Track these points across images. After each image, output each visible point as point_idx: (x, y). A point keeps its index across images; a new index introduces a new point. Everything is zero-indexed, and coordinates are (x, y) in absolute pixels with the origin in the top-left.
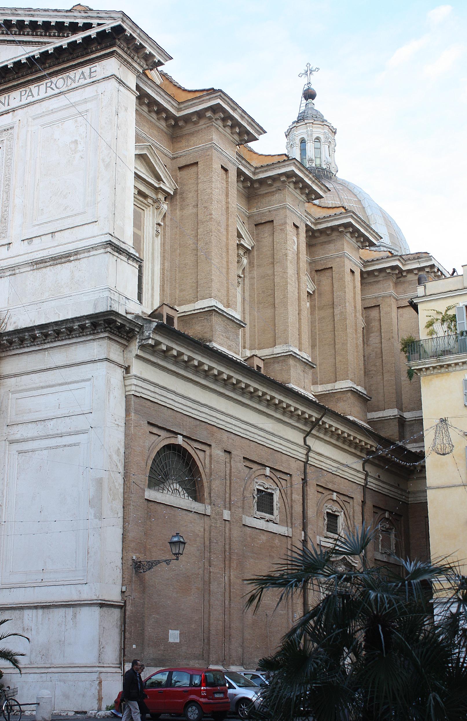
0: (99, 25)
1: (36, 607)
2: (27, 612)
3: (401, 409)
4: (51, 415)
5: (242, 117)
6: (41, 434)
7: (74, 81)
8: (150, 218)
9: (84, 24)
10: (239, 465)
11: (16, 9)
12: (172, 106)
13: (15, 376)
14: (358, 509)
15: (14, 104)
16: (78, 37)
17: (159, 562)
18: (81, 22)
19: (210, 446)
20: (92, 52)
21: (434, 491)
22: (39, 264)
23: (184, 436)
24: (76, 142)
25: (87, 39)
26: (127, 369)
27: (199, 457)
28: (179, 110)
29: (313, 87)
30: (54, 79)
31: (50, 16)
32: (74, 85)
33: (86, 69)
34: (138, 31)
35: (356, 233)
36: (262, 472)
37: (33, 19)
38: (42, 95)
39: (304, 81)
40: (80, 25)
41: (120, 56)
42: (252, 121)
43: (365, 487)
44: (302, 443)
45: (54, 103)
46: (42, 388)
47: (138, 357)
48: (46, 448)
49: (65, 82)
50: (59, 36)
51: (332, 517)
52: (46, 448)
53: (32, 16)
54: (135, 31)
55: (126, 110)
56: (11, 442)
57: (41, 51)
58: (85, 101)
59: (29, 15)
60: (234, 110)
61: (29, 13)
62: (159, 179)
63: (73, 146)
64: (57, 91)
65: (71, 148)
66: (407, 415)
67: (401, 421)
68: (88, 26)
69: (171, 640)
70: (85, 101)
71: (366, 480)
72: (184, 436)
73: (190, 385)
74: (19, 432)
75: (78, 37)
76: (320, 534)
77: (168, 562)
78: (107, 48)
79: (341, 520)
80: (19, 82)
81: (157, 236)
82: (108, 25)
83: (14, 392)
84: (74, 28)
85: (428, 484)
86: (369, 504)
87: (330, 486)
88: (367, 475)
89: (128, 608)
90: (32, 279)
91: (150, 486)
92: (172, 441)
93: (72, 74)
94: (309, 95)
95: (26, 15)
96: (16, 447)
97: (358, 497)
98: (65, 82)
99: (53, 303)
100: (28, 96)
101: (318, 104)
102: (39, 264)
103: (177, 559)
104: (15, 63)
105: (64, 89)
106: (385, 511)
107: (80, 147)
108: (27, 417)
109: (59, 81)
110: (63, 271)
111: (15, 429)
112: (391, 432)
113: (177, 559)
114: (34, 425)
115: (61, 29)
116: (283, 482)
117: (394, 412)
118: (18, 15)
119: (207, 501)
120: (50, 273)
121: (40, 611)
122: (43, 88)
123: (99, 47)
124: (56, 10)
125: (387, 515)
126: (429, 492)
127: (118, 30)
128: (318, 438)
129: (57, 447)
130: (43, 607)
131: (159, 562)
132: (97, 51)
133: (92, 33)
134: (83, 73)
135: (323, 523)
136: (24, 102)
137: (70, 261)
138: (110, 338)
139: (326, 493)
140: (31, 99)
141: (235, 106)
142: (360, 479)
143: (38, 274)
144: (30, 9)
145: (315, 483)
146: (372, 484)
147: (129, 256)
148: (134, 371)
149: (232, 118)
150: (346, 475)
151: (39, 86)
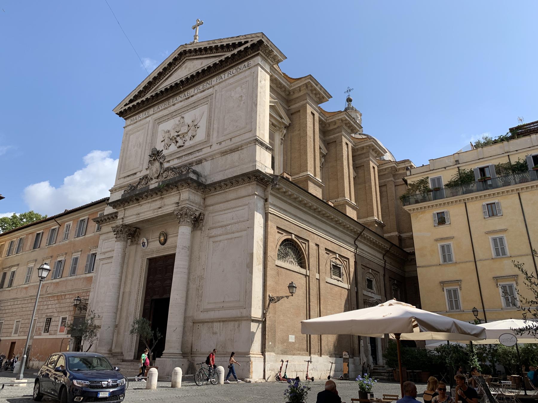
1: (220, 321)
2: (215, 324)
3: (399, 232)
4: (229, 222)
5: (321, 89)
7: (241, 69)
8: (278, 138)
10: (322, 252)
11: (214, 40)
12: (288, 85)
13: (212, 205)
14: (382, 278)
15: (213, 83)
16: (242, 48)
17: (282, 297)
18: (243, 41)
19: (308, 241)
21: (420, 269)
22: (224, 153)
23: (295, 235)
24: (241, 96)
25: (246, 48)
26: (266, 200)
27: (303, 246)
28: (291, 86)
29: (351, 98)
30: (231, 70)
32: (241, 71)
33: (246, 63)
34: (270, 43)
35: (374, 150)
36: (335, 256)
37: (222, 44)
38: (226, 77)
39: (347, 94)
41: (262, 56)
42: (325, 92)
43: (384, 268)
44: (353, 243)
45: (231, 81)
46: (225, 210)
47: (271, 194)
48: (226, 240)
51: (370, 282)
52: (226, 240)
53: (222, 42)
54: (268, 43)
55: (265, 80)
56: (210, 237)
58: (246, 77)
60: (317, 85)
62: (281, 118)
63: (240, 98)
64: (233, 75)
66: (404, 235)
67: (400, 239)
68: (246, 42)
69: (290, 340)
70: (246, 77)
71: (385, 264)
72: (295, 235)
73: (298, 211)
74: (214, 232)
75: (242, 48)
76: (365, 290)
77: (287, 297)
78: (255, 51)
79: (374, 283)
81: (281, 144)
82: (256, 40)
83: (212, 213)
84: (240, 44)
85: (418, 264)
86: (387, 276)
87: (368, 266)
88: (385, 262)
89: (267, 322)
90: (221, 161)
91: (279, 259)
92: (290, 237)
93: (240, 67)
94: (349, 100)
96: (212, 239)
97: (382, 272)
99: (231, 170)
101: (353, 104)
102: (224, 153)
103: (292, 295)
105: (236, 73)
106: (395, 280)
107: (243, 98)
108: (217, 225)
109: (234, 71)
110: (235, 156)
111: (212, 231)
112: (396, 242)
113: (292, 295)
114: (221, 228)
115: (234, 46)
116: (345, 262)
117: (397, 233)
119: (307, 268)
120: (229, 157)
121: (222, 323)
122: (226, 75)
124: (232, 38)
125: (395, 282)
126: (418, 269)
127: (261, 42)
128: (361, 242)
129: (231, 239)
130: (223, 321)
131: (282, 297)
132: (251, 54)
133: (248, 45)
135: (365, 284)
136: (218, 81)
137: (238, 150)
138: (257, 184)
139: (366, 269)
140: (221, 80)
141: (317, 83)
142: (382, 263)
143: (224, 158)
144: (220, 39)
145: (360, 264)
146: (388, 266)
147: (267, 148)
148: (270, 200)
149: (315, 89)
150: (376, 261)
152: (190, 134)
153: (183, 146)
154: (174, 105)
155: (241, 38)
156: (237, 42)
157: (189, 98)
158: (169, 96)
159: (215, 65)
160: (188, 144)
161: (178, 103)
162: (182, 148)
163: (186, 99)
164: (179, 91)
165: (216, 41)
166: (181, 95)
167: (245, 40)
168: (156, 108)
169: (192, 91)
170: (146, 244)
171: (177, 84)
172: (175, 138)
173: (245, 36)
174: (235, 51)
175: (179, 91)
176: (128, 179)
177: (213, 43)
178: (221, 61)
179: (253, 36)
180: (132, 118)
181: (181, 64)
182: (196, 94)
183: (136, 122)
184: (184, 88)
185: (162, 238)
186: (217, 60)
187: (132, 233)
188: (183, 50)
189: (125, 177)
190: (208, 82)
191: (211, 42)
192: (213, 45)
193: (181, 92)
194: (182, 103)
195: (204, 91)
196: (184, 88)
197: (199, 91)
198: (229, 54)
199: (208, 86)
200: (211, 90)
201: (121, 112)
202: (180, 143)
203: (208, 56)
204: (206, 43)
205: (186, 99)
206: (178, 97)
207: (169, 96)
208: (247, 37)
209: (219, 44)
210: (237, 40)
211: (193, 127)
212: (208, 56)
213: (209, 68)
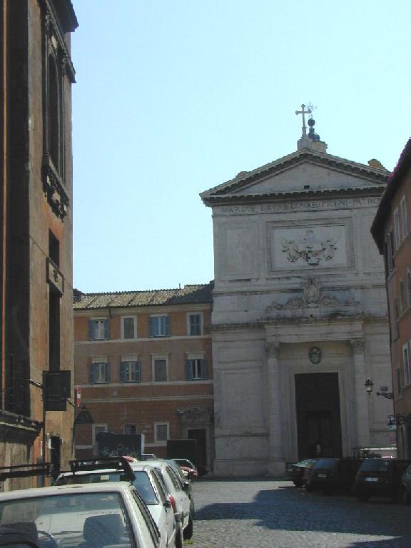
13: (372, 334)
15: (350, 206)
152: (326, 253)
153: (316, 264)
160: (324, 263)
161: (301, 211)
162: (316, 267)
168: (265, 206)
169: (320, 204)
172: (307, 254)
176: (238, 284)
180: (225, 207)
187: (282, 349)
189: (231, 281)
190: (342, 200)
197: (329, 207)
199: (342, 206)
200: (347, 213)
202: (313, 260)
211: (329, 248)
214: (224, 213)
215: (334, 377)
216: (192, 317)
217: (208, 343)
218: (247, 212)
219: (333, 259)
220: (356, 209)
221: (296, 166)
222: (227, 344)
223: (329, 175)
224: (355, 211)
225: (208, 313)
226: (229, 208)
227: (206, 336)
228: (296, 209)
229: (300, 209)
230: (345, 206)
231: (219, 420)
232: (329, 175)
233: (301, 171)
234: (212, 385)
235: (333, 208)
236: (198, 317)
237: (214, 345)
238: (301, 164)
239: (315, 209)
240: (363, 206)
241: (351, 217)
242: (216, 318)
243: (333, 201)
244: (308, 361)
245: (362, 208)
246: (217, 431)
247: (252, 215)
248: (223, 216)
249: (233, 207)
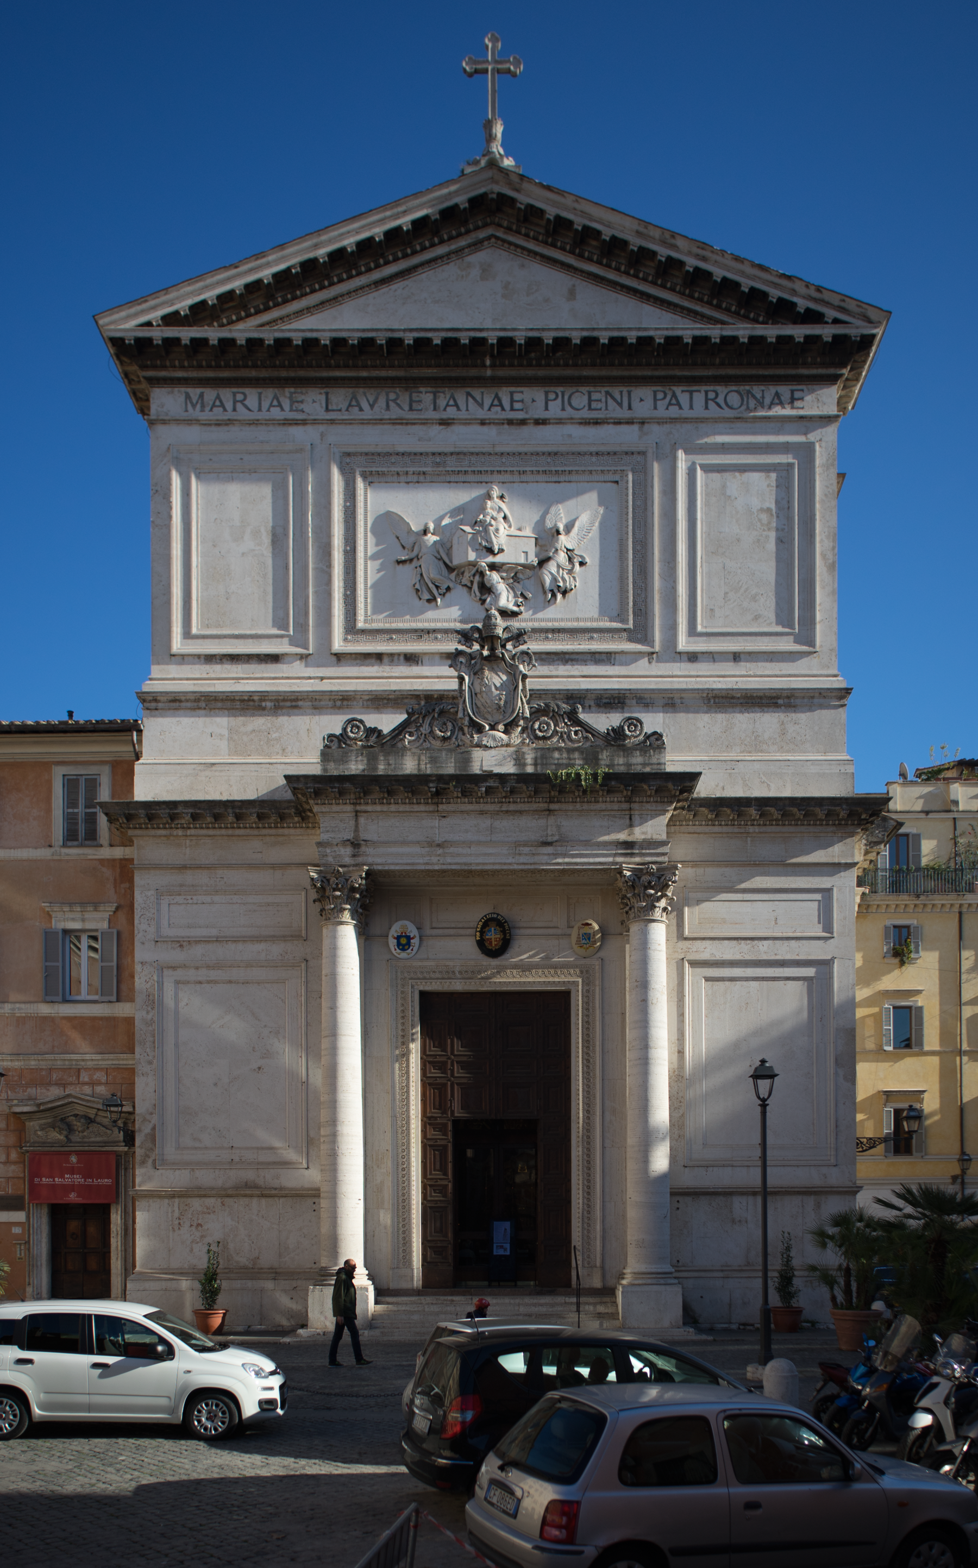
0: (836, 321)
6: (747, 957)
9: (808, 310)
11: (673, 235)
16: (799, 332)
18: (802, 304)
20: (805, 365)
31: (743, 273)
38: (699, 410)
40: (801, 310)
49: (742, 400)
50: (737, 313)
53: (704, 259)
57: (698, 333)
59: (697, 256)
61: (700, 252)
65: (760, 520)
68: (812, 317)
80: (657, 373)
84: (783, 310)
95: (690, 253)
98: (742, 400)
100: (670, 404)
104: (667, 339)
115: (753, 303)
118: (674, 247)
122: (699, 398)
123: (819, 360)
124: (761, 267)
133: (826, 332)
134: (777, 395)
140: (674, 412)
144: (704, 245)
151: (691, 393)
154: (445, 423)
155: (798, 286)
156: (775, 294)
157: (523, 422)
158: (415, 372)
159: (673, 342)
161: (467, 422)
163: (510, 422)
164: (473, 372)
165: (680, 242)
166: (476, 393)
167: (812, 306)
168: (340, 397)
169: (533, 400)
170: (415, 942)
171: (478, 343)
173: (819, 289)
174: (771, 332)
175: (473, 372)
177: (663, 242)
178: (700, 341)
179: (851, 306)
180: (195, 392)
181: (462, 242)
182: (560, 422)
183: (229, 422)
184: (501, 373)
185: (494, 936)
186: (687, 329)
188: (497, 188)
190: (616, 392)
191: (656, 234)
192: (663, 252)
193: (479, 381)
194: (491, 432)
195: (597, 422)
196: (501, 373)
197: (569, 412)
198: (743, 331)
200: (627, 436)
201: (143, 344)
203: (612, 276)
204: (628, 223)
205: (510, 422)
206: (461, 397)
207: (415, 372)
208: (826, 296)
209: (691, 263)
210: (776, 285)
212: (612, 276)
213: (644, 342)
214: (196, 413)
215: (555, 1005)
216: (71, 784)
217: (125, 872)
218: (276, 413)
219: (570, 596)
220: (661, 422)
221: (459, 252)
222: (189, 878)
223: (572, 294)
224: (656, 431)
225: (124, 771)
226: (210, 394)
227: (119, 853)
228: (451, 412)
229: (463, 415)
230: (624, 414)
231: (152, 1137)
232: (572, 294)
233: (475, 272)
234: (130, 1021)
235: (585, 414)
236: (93, 784)
237: (139, 879)
238: (477, 246)
239: (520, 415)
240: (686, 413)
241: (643, 453)
242: (147, 787)
243: (584, 389)
244: (467, 948)
245: (685, 420)
246: (145, 1179)
247: (295, 422)
248: (189, 422)
249: (226, 394)
